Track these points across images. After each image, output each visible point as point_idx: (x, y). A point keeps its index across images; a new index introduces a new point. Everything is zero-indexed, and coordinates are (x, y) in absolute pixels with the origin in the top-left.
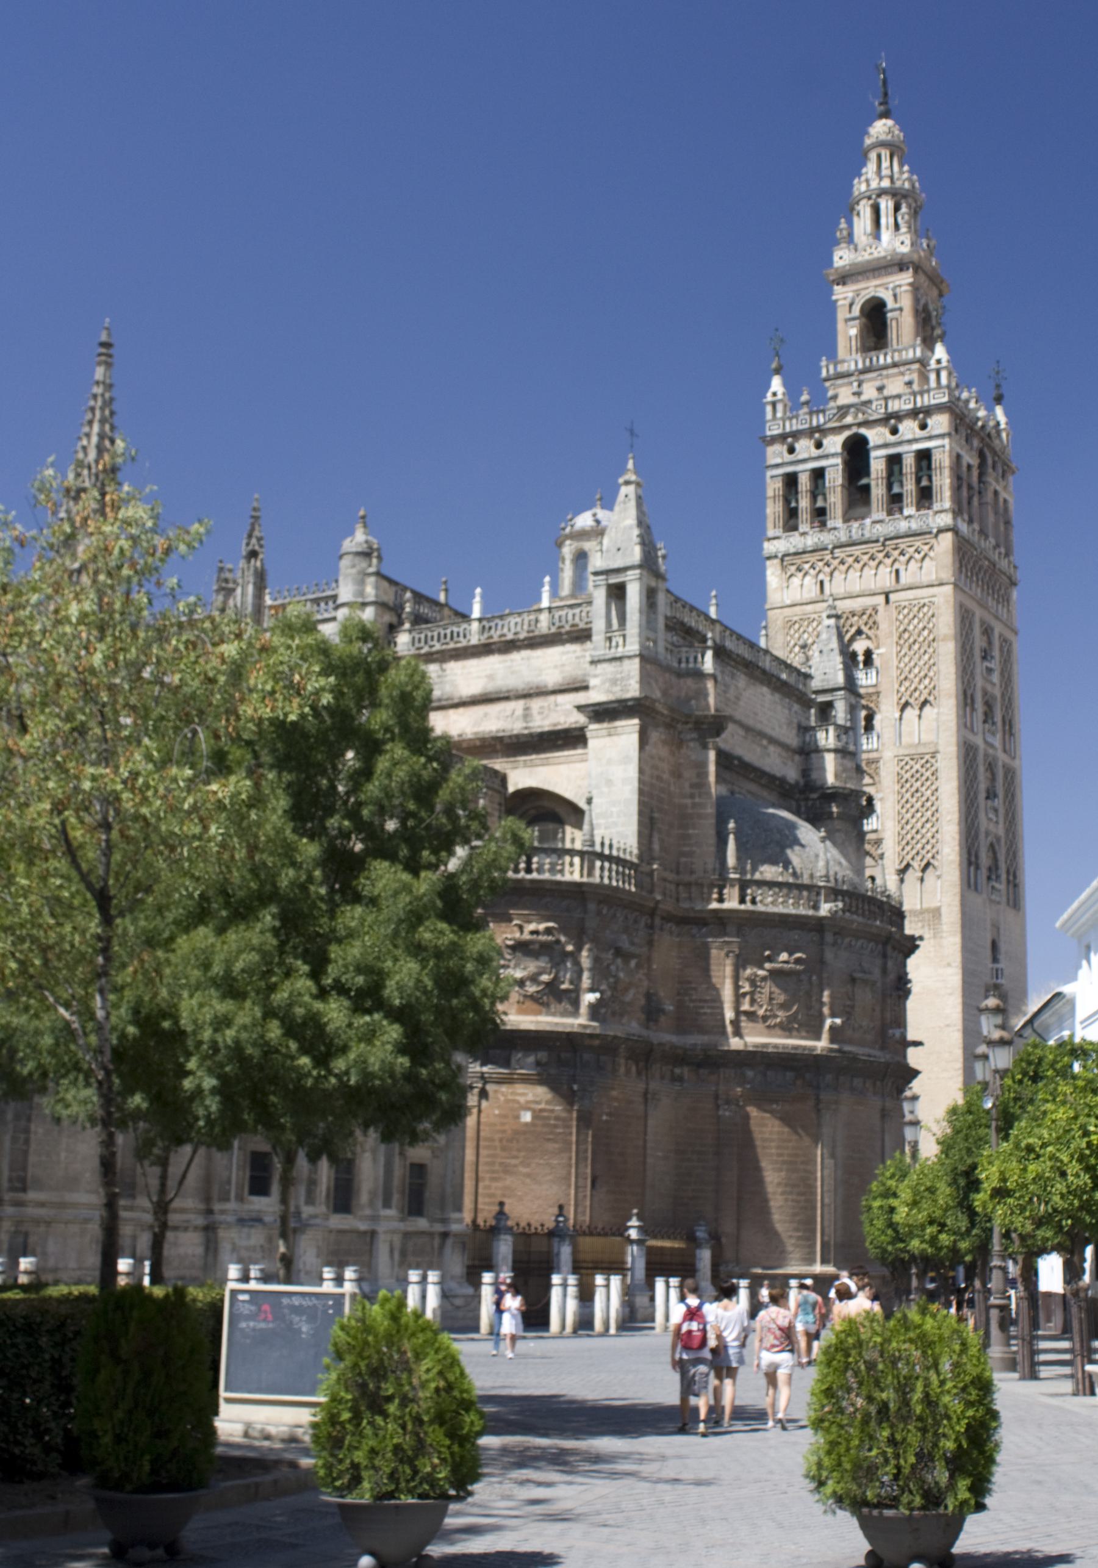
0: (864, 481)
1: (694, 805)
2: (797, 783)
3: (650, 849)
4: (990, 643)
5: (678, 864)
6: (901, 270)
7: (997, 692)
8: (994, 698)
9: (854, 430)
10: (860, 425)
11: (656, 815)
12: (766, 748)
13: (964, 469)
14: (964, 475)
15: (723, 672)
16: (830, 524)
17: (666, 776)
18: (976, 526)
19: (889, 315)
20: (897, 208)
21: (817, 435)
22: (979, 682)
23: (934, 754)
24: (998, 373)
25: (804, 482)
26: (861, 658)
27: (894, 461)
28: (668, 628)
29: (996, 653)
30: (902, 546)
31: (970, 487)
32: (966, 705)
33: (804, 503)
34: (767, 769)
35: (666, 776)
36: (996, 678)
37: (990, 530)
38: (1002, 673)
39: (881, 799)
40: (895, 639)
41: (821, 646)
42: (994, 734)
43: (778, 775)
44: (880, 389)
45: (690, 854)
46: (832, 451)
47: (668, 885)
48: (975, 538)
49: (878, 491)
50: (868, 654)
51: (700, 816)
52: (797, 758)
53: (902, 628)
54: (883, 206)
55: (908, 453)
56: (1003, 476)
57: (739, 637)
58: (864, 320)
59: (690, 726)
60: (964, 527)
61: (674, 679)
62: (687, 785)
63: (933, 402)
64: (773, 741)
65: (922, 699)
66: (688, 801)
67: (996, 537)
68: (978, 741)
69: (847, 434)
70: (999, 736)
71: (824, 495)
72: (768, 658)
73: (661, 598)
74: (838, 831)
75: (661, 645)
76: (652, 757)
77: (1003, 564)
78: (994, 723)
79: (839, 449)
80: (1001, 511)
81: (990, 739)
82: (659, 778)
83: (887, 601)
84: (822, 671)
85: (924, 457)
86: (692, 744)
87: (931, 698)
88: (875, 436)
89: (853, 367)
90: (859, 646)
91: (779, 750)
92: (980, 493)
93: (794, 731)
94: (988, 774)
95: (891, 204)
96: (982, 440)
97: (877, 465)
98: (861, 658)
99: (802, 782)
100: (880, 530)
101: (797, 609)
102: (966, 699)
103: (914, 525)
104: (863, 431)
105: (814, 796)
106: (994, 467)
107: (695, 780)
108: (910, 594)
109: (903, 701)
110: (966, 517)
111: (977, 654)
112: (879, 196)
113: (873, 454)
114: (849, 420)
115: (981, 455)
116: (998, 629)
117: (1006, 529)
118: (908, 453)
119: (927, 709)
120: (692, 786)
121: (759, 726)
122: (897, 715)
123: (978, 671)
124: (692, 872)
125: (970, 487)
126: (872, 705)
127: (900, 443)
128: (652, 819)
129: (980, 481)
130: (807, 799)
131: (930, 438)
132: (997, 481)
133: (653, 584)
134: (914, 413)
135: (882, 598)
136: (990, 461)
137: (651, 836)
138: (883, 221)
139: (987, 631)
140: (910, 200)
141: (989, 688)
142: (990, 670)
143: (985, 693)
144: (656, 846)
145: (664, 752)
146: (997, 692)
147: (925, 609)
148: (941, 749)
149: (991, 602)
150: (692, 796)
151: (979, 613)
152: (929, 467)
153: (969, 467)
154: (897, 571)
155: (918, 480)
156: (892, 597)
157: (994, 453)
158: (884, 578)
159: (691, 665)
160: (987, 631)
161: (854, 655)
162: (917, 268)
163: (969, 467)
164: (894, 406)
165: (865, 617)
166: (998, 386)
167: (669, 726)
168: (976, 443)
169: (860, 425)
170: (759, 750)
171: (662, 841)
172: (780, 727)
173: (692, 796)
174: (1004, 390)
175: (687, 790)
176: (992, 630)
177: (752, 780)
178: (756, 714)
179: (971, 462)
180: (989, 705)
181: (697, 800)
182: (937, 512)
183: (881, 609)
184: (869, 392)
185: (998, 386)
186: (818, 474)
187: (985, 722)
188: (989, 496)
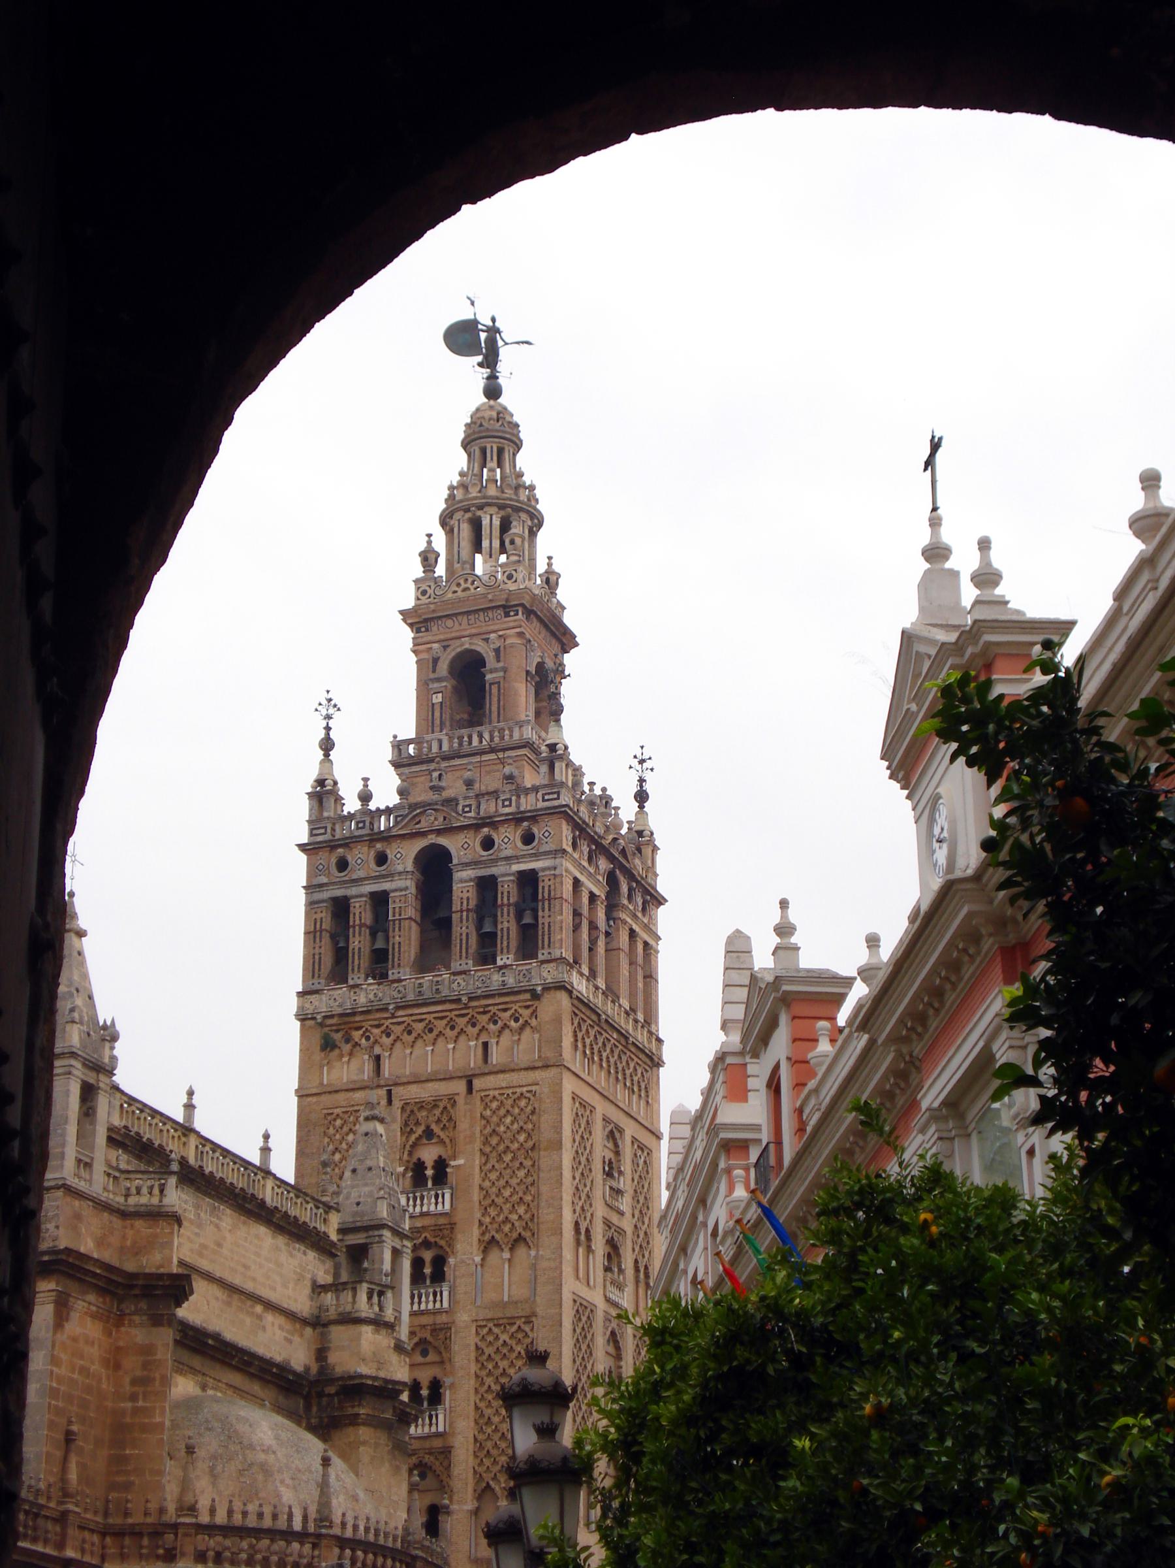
0: (442, 914)
1: (136, 1411)
2: (307, 1369)
3: (64, 1480)
4: (617, 1153)
5: (107, 1501)
6: (507, 615)
7: (627, 1224)
8: (621, 1231)
9: (432, 839)
11: (75, 1428)
12: (260, 1317)
13: (585, 900)
14: (585, 910)
15: (197, 1207)
16: (392, 974)
17: (95, 1367)
18: (601, 983)
19: (488, 677)
20: (505, 526)
21: (379, 846)
22: (600, 1211)
23: (528, 1321)
24: (642, 762)
25: (361, 913)
26: (429, 1172)
27: (487, 885)
28: (112, 1141)
29: (627, 1166)
30: (493, 1009)
31: (593, 926)
32: (578, 1243)
33: (359, 942)
34: (260, 1350)
35: (95, 1367)
36: (625, 1204)
37: (624, 988)
38: (635, 1197)
39: (452, 1386)
40: (478, 1145)
41: (353, 1163)
42: (620, 1287)
43: (278, 1358)
44: (469, 783)
45: (127, 1487)
46: (400, 868)
47: (86, 1534)
48: (598, 1001)
49: (463, 929)
50: (441, 1165)
51: (144, 1428)
52: (308, 1331)
53: (488, 1130)
54: (486, 522)
55: (506, 872)
56: (644, 910)
57: (226, 1152)
58: (454, 682)
59: (136, 1291)
60: (581, 986)
61: (117, 1222)
62: (127, 1380)
63: (541, 805)
64: (270, 1306)
65: (515, 1235)
66: (129, 1405)
67: (632, 995)
68: (596, 1297)
69: (421, 843)
70: (629, 1289)
71: (386, 931)
72: (270, 1183)
73: (103, 1103)
74: (364, 1443)
75: (99, 1167)
76: (75, 1339)
77: (641, 1037)
78: (621, 1271)
79: (410, 866)
80: (640, 960)
81: (614, 1295)
82: (83, 1370)
83: (470, 1089)
84: (353, 1199)
85: (529, 880)
86: (136, 1318)
87: (527, 1234)
88: (460, 847)
89: (435, 749)
90: (429, 1154)
91: (281, 1320)
92: (607, 934)
93: (307, 1291)
94: (611, 1349)
95: (497, 522)
96: (611, 858)
98: (429, 1172)
99: (314, 1369)
100: (462, 986)
101: (341, 1097)
102: (583, 1237)
104: (443, 841)
105: (331, 1390)
106: (630, 898)
107: (138, 1373)
108: (502, 1080)
109: (487, 1237)
110: (586, 971)
111: (597, 1166)
112: (481, 507)
113: (458, 875)
114: (424, 825)
115: (612, 880)
116: (630, 1130)
117: (645, 984)
118: (506, 872)
119: (521, 1251)
120: (135, 1382)
121: (249, 1286)
122: (478, 1259)
123: (598, 1194)
124: (127, 1514)
125: (593, 926)
126: (442, 1243)
127: (494, 861)
128: (69, 1438)
129: (609, 917)
130: (321, 1395)
131: (536, 856)
132: (635, 916)
133: (92, 1081)
134: (517, 819)
135: (460, 1087)
136: (624, 888)
137: (65, 1459)
139: (614, 1135)
140: (524, 516)
141: (615, 1219)
142: (618, 1192)
143: (608, 1224)
144: (73, 1476)
145: (93, 1329)
146: (627, 1224)
147: (523, 1103)
148: (540, 1311)
149: (621, 1095)
150: (133, 1397)
151: (601, 1108)
152: (535, 897)
153: (593, 897)
154: (486, 1045)
155: (519, 916)
156: (477, 1083)
157: (631, 876)
158: (466, 1053)
159: (144, 1200)
160: (614, 1135)
161: (419, 1167)
162: (529, 613)
163: (593, 897)
164: (488, 807)
165: (437, 1112)
166: (642, 781)
167: (102, 1291)
168: (603, 864)
169: (439, 832)
170: (248, 1320)
171: (82, 1467)
172: (285, 1286)
173: (133, 1397)
174: (648, 787)
175: (128, 1388)
176: (621, 1131)
177: (237, 1369)
178: (246, 1267)
179: (596, 891)
180: (613, 1247)
181: (140, 1403)
182: (543, 962)
183: (461, 1100)
184: (454, 787)
185: (642, 781)
186: (380, 900)
187: (607, 1269)
188: (624, 937)
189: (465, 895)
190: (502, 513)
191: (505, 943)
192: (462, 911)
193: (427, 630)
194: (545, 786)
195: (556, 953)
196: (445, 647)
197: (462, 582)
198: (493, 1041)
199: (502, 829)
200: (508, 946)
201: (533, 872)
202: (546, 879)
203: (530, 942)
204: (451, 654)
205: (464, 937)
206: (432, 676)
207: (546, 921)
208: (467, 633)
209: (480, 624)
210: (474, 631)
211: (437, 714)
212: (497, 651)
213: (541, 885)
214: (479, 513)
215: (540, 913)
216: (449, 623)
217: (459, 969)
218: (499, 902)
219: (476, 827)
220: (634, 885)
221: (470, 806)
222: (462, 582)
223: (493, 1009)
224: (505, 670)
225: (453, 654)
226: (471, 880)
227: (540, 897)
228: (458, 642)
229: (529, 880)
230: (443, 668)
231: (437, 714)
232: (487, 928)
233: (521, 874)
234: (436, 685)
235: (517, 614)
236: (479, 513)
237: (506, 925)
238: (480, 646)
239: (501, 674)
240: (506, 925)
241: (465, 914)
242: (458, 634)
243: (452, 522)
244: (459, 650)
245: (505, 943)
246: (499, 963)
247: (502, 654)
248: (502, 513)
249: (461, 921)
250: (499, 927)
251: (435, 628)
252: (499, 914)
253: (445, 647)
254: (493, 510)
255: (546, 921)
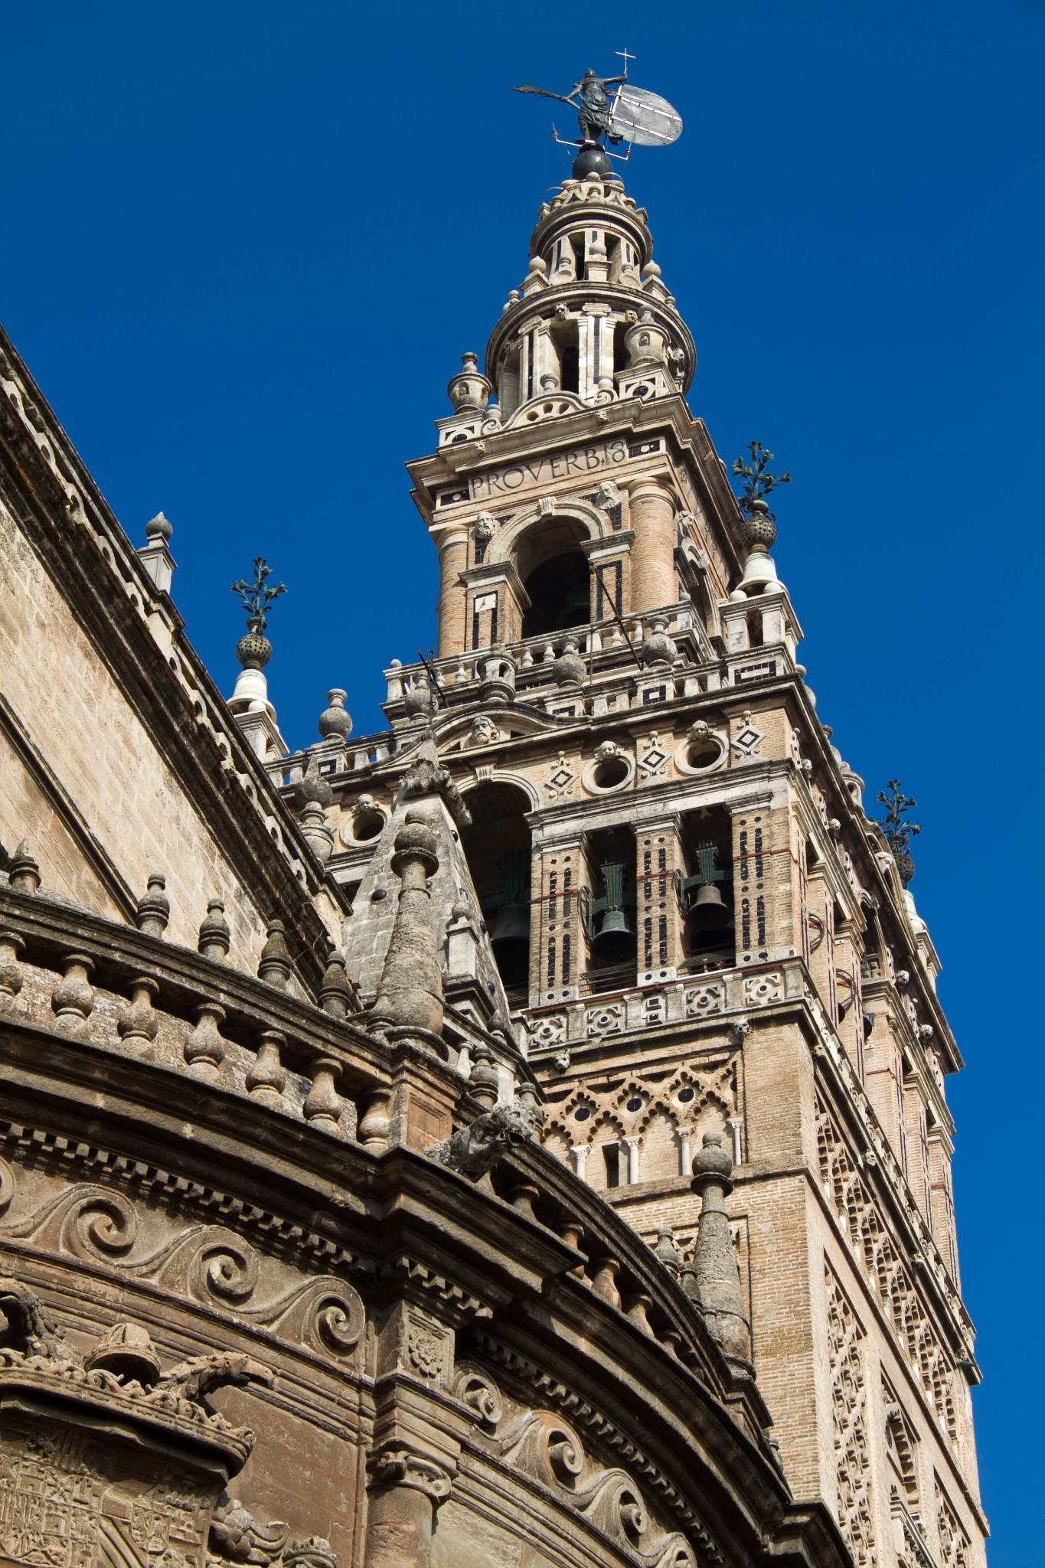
6: (635, 452)
10: (502, 757)
19: (595, 556)
27: (611, 849)
54: (586, 329)
85: (707, 830)
95: (608, 333)
97: (557, 862)
103: (671, 1012)
112: (576, 305)
131: (725, 778)
138: (585, 362)
169: (502, 757)
189: (561, 867)
190: (620, 317)
191: (656, 947)
192: (553, 897)
193: (466, 496)
194: (741, 655)
195: (777, 952)
196: (502, 521)
197: (539, 410)
198: (631, 1139)
199: (641, 743)
200: (663, 952)
201: (720, 816)
202: (750, 819)
203: (712, 936)
204: (514, 529)
205: (559, 944)
206: (472, 566)
207: (753, 896)
208: (553, 488)
209: (578, 469)
210: (564, 486)
211: (485, 630)
212: (615, 513)
213: (737, 831)
214: (570, 316)
215: (738, 883)
216: (513, 478)
217: (546, 1002)
218: (641, 871)
219: (583, 742)
220: (906, 975)
221: (571, 710)
222: (539, 410)
223: (630, 1078)
224: (629, 538)
225: (521, 527)
226: (575, 837)
227: (736, 853)
228: (533, 507)
229: (707, 830)
230: (499, 551)
231: (485, 630)
232: (616, 924)
233: (690, 819)
234: (482, 582)
235: (657, 448)
236: (570, 316)
237: (656, 912)
238: (577, 509)
239: (625, 547)
240: (656, 912)
241: (560, 901)
242: (530, 494)
243: (513, 346)
244: (535, 519)
245: (656, 947)
246: (642, 982)
247: (626, 515)
248: (620, 317)
249: (552, 915)
250: (642, 916)
251: (479, 491)
252: (641, 893)
253: (502, 521)
254: (602, 308)
255: (753, 896)
